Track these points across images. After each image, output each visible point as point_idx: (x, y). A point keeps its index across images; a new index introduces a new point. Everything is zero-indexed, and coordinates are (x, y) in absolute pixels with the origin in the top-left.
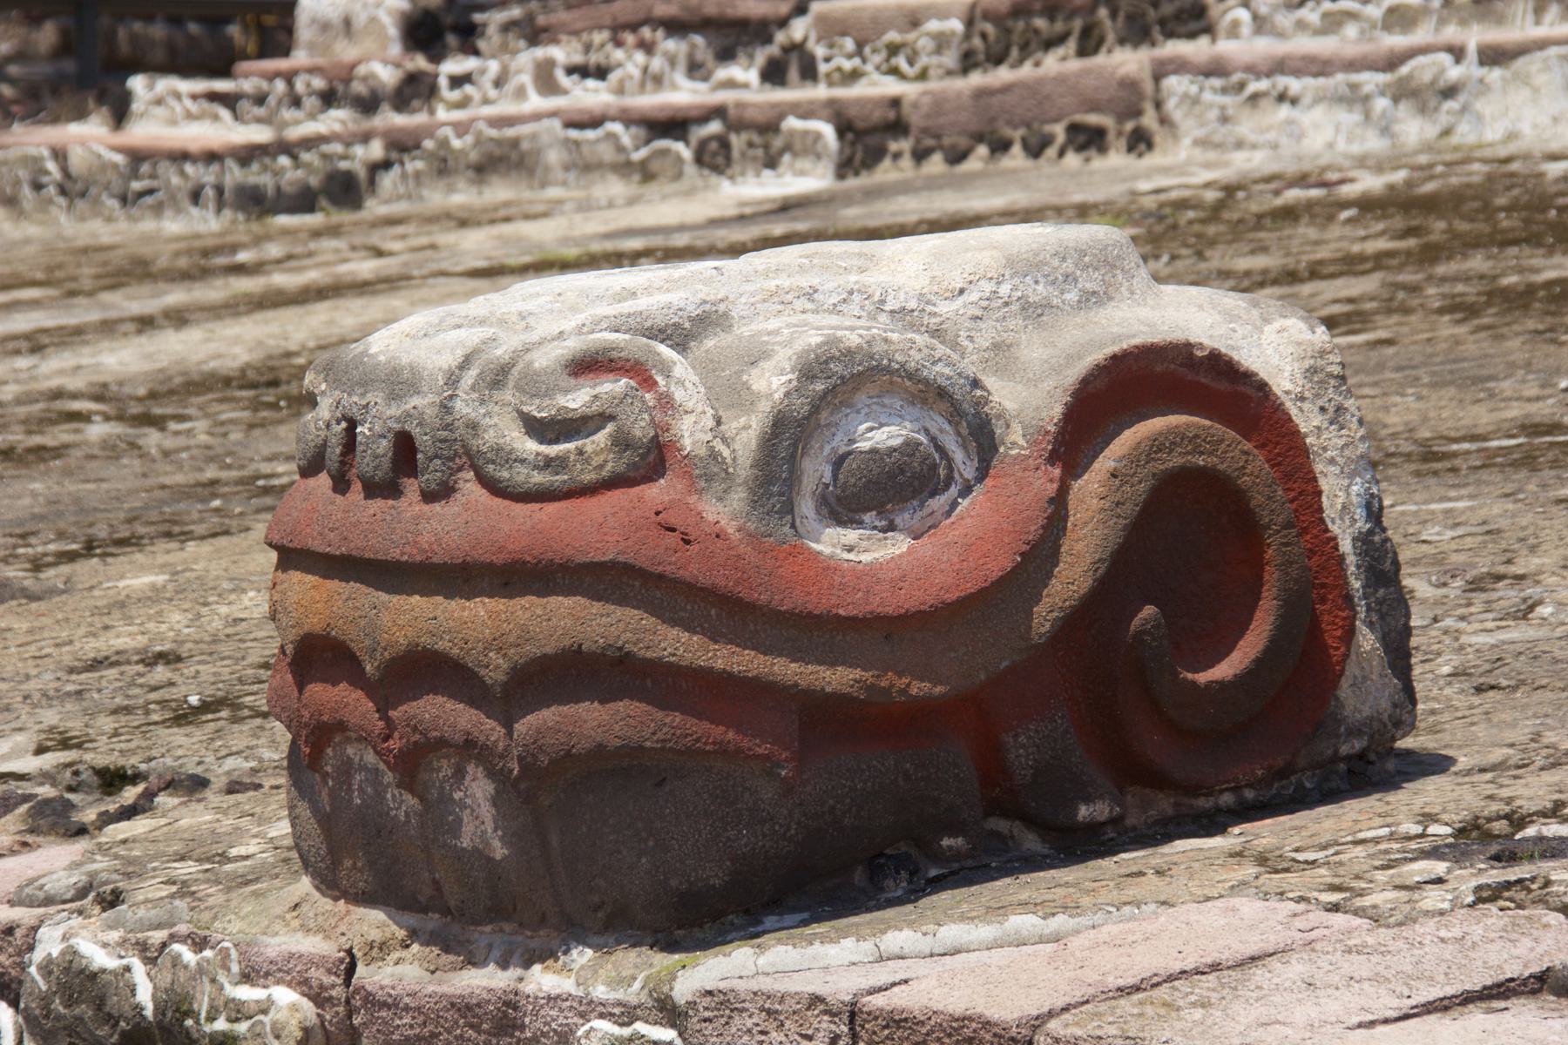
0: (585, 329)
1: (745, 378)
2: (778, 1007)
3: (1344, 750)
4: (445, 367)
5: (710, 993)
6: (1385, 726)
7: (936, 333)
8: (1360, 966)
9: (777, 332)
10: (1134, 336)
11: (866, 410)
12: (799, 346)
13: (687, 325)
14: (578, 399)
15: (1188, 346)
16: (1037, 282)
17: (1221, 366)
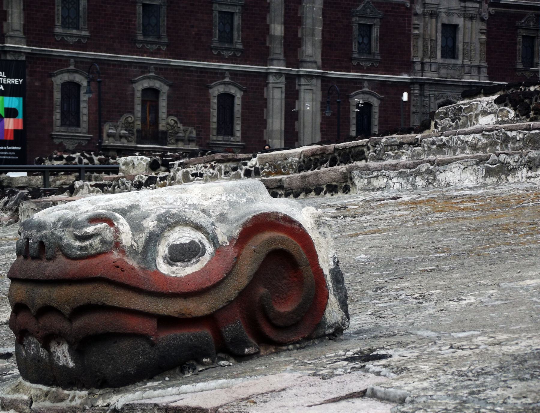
0: (95, 210)
1: (142, 223)
2: (146, 408)
3: (327, 332)
4: (53, 221)
5: (127, 405)
6: (340, 325)
7: (204, 211)
8: (312, 390)
9: (153, 210)
10: (261, 211)
11: (179, 232)
12: (158, 213)
13: (126, 208)
14: (90, 229)
15: (277, 213)
16: (233, 196)
17: (287, 219)
